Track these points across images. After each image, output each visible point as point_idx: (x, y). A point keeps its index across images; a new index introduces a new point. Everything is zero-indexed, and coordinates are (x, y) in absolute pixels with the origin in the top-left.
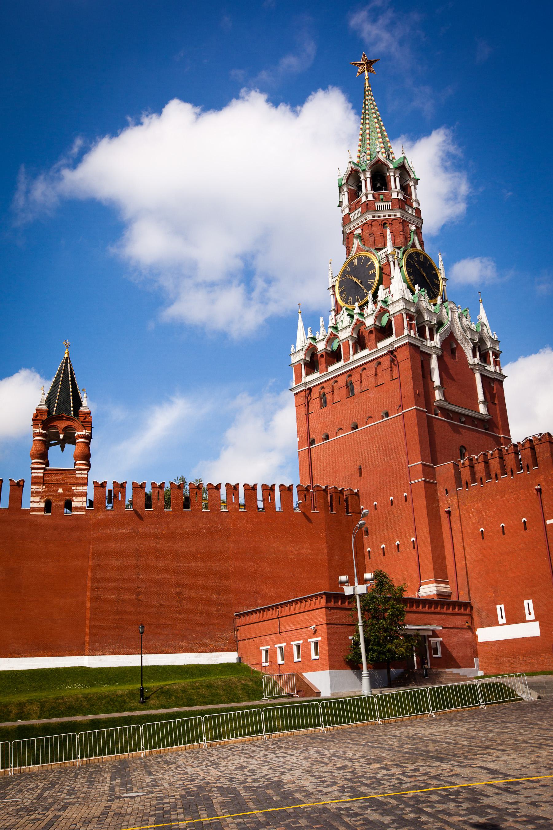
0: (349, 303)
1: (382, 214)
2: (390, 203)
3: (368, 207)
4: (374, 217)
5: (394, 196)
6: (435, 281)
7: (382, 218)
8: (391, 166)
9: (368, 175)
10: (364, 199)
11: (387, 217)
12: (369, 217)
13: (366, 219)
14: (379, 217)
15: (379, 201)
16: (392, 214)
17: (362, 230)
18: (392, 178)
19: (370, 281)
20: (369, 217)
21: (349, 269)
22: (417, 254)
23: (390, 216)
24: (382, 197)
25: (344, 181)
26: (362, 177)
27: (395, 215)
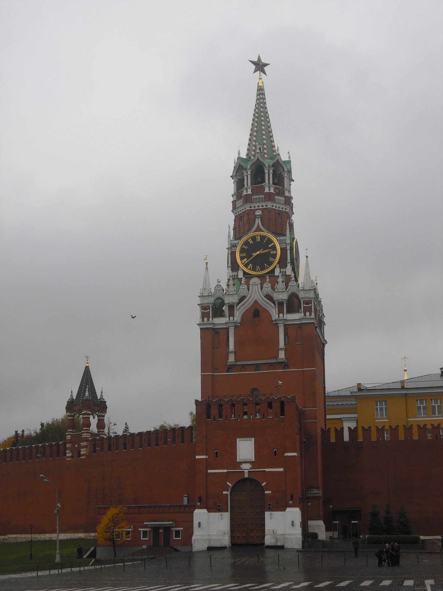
0: (249, 268)
1: (278, 206)
2: (283, 199)
3: (269, 197)
5: (287, 194)
8: (286, 170)
9: (271, 171)
10: (267, 190)
12: (270, 205)
13: (266, 206)
15: (277, 195)
17: (262, 212)
18: (285, 178)
19: (271, 259)
20: (270, 205)
21: (251, 242)
24: (277, 191)
26: (266, 171)
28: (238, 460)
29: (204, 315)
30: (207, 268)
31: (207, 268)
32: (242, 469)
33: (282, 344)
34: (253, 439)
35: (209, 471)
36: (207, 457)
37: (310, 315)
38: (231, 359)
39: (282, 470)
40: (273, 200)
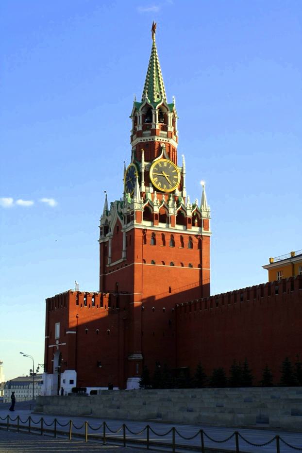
2: (150, 132)
4: (141, 141)
5: (153, 127)
6: (175, 177)
7: (146, 141)
11: (148, 141)
12: (138, 140)
14: (144, 140)
16: (151, 138)
20: (138, 140)
22: (162, 163)
23: (150, 139)
25: (133, 115)
27: (153, 139)
28: (56, 338)
29: (101, 233)
30: (106, 199)
31: (106, 199)
32: (56, 344)
33: (124, 248)
34: (59, 323)
35: (50, 346)
36: (49, 337)
37: (133, 222)
38: (109, 260)
39: (65, 344)
40: (142, 136)
